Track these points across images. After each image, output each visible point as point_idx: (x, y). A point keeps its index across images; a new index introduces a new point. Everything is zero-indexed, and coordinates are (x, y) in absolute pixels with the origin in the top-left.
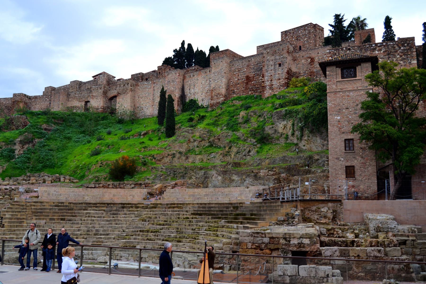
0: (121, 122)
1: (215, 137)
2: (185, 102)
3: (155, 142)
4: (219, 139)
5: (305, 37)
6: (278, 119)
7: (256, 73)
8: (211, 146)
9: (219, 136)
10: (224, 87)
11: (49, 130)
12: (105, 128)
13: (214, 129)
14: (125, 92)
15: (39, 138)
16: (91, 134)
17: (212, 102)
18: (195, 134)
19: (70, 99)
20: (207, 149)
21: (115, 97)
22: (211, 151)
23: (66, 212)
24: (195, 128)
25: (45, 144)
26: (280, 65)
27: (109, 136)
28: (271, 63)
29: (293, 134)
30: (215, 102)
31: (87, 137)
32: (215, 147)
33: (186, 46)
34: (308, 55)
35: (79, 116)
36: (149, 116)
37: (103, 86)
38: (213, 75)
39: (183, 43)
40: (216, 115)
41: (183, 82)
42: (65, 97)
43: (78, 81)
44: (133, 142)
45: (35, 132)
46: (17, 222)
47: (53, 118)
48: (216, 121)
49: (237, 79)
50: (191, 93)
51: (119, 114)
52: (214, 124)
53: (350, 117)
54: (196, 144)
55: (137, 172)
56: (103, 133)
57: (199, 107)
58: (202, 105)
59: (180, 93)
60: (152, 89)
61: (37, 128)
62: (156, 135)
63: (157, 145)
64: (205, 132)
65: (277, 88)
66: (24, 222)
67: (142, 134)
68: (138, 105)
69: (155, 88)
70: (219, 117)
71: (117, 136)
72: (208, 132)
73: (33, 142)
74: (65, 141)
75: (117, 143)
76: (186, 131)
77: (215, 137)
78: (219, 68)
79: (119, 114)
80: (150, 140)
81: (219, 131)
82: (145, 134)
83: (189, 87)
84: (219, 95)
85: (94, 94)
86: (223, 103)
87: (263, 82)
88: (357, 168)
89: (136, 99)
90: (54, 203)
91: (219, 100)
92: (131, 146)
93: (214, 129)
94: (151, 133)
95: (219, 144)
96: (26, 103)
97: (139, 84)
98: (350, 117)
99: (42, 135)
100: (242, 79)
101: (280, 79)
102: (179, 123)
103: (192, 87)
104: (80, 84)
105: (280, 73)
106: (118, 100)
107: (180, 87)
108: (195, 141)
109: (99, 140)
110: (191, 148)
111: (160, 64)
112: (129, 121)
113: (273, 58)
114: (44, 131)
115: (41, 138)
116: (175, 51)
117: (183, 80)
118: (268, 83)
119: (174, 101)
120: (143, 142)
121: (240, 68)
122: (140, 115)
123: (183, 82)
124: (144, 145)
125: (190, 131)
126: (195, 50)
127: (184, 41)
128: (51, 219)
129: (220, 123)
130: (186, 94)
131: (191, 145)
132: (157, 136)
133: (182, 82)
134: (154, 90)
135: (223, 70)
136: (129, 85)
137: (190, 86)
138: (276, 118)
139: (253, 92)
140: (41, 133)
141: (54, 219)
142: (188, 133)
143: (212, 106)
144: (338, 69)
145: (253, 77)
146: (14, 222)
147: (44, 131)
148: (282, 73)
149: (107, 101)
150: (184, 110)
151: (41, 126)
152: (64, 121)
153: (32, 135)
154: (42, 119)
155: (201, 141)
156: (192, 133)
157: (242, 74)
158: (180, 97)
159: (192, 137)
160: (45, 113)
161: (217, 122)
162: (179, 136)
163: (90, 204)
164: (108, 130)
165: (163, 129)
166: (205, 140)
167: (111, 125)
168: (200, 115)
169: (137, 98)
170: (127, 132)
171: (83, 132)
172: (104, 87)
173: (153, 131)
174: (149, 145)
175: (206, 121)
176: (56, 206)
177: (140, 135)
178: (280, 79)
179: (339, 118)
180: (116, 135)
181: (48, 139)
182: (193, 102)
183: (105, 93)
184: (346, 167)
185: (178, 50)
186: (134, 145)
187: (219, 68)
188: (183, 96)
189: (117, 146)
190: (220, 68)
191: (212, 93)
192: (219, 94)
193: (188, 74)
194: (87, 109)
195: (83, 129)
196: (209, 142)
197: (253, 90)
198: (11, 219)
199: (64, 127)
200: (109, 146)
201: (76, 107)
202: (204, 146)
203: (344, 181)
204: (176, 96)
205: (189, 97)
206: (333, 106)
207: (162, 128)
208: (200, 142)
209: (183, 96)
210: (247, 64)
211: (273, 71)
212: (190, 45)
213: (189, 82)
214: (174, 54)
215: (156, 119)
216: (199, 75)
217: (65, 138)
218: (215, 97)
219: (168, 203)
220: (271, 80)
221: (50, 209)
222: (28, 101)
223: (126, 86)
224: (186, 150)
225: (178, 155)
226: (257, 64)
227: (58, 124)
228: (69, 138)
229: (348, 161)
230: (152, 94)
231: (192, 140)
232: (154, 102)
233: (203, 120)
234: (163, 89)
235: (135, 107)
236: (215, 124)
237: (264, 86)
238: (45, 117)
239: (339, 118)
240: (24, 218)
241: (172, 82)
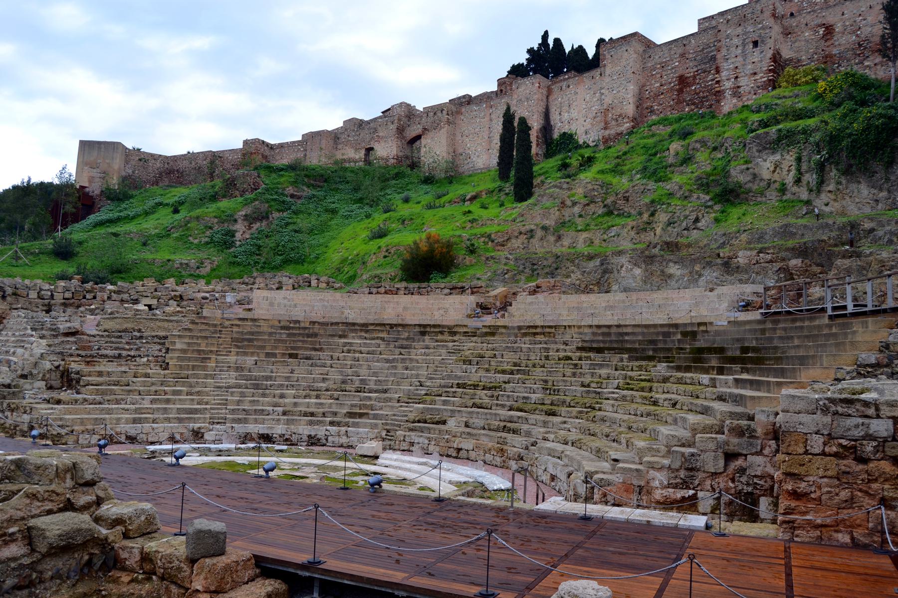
0: (429, 180)
1: (617, 195)
2: (551, 138)
3: (493, 211)
4: (627, 199)
6: (759, 151)
7: (699, 67)
8: (610, 213)
9: (627, 192)
10: (631, 101)
11: (299, 198)
12: (399, 193)
13: (615, 181)
14: (436, 126)
15: (279, 211)
16: (374, 203)
17: (607, 132)
18: (574, 191)
19: (340, 146)
20: (600, 220)
21: (418, 137)
22: (610, 224)
23: (303, 341)
24: (574, 180)
25: (290, 221)
26: (755, 44)
27: (406, 206)
28: (736, 41)
29: (798, 181)
30: (613, 132)
31: (367, 208)
32: (618, 215)
33: (551, 42)
34: (819, 21)
35: (352, 171)
36: (481, 169)
37: (396, 118)
38: (607, 79)
39: (545, 36)
40: (616, 155)
41: (547, 101)
42: (331, 142)
43: (357, 119)
44: (451, 213)
45: (273, 200)
46: (196, 359)
47: (306, 176)
48: (618, 165)
49: (658, 85)
50: (563, 120)
51: (426, 166)
52: (613, 171)
54: (577, 210)
55: (457, 267)
56: (397, 199)
57: (578, 147)
58: (584, 143)
59: (542, 122)
60: (487, 119)
61: (276, 193)
62: (495, 198)
63: (498, 216)
64: (596, 187)
65: (750, 93)
66: (210, 358)
67: (468, 198)
68: (461, 151)
69: (493, 116)
70: (624, 157)
71: (420, 205)
72: (602, 187)
73: (268, 218)
74: (325, 217)
75: (419, 215)
76: (555, 186)
77: (617, 195)
78: (622, 64)
79: (426, 166)
80: (484, 207)
81: (627, 184)
82: (473, 198)
83: (558, 110)
85: (381, 134)
86: (630, 133)
87: (718, 82)
89: (457, 139)
90: (279, 321)
91: (622, 129)
92: (445, 219)
93: (615, 181)
94: (484, 196)
95: (626, 209)
96: (265, 157)
97: (463, 110)
99: (284, 206)
100: (670, 83)
101: (755, 74)
102: (540, 175)
103: (565, 108)
104: (361, 125)
105: (756, 60)
106: (423, 141)
107: (542, 109)
108: (574, 204)
109: (386, 212)
110: (567, 219)
111: (505, 74)
112: (445, 178)
113: (739, 30)
114: (289, 199)
115: (283, 211)
116: (530, 51)
117: (547, 97)
118: (728, 85)
119: (530, 129)
120: (469, 212)
121: (665, 62)
122: (465, 168)
123: (547, 101)
124: (470, 217)
125: (565, 186)
126: (568, 49)
127: (546, 33)
128: (268, 355)
129: (625, 168)
130: (552, 123)
131: (567, 213)
132: (496, 200)
133: (545, 100)
134: (491, 120)
135: (629, 68)
136: (445, 112)
137: (561, 107)
138: (754, 150)
139: (693, 107)
140: (283, 202)
141: (274, 355)
142: (561, 188)
143: (606, 140)
145: (694, 77)
146: (189, 359)
147: (289, 199)
148: (761, 61)
149: (405, 146)
150: (548, 155)
151: (284, 189)
152: (325, 181)
153: (267, 205)
154: (288, 177)
155: (588, 205)
156: (569, 189)
157: (669, 72)
158: (541, 129)
159: (569, 197)
160: (292, 167)
161: (619, 168)
162: (542, 196)
163: (354, 324)
164: (406, 193)
165: (509, 187)
166: (595, 202)
167: (410, 186)
168: (583, 157)
169: (459, 137)
170: (439, 197)
171: (360, 200)
172: (399, 120)
173: (490, 192)
174: (481, 217)
175: (595, 168)
176: (283, 328)
177: (464, 201)
178: (755, 74)
180: (419, 203)
181: (296, 213)
182: (568, 141)
183: (401, 131)
185: (536, 49)
186: (453, 216)
187: (622, 64)
188: (547, 128)
189: (419, 221)
190: (624, 63)
191: (606, 116)
192: (620, 116)
193: (557, 85)
194: (367, 161)
195: (359, 195)
196: (605, 206)
197: (694, 104)
198: (184, 351)
199: (325, 191)
200: (404, 221)
201: (349, 161)
202: (594, 213)
204: (535, 124)
205: (559, 127)
207: (508, 185)
208: (585, 206)
209: (547, 128)
210: (680, 51)
211: (740, 59)
212: (557, 41)
213: (558, 98)
214: (528, 56)
215: (494, 173)
216: (579, 83)
217: (327, 211)
218: (614, 123)
219: (522, 324)
220: (737, 77)
221: (270, 334)
222: (267, 153)
223: (439, 114)
224: (556, 223)
225: (539, 233)
226: (703, 49)
227: (314, 187)
228: (334, 212)
230: (486, 129)
231: (569, 203)
232: (490, 142)
233: (589, 166)
234: (508, 109)
235: (455, 154)
236: (616, 171)
237: (719, 92)
238: (293, 174)
240: (211, 351)
241: (528, 101)
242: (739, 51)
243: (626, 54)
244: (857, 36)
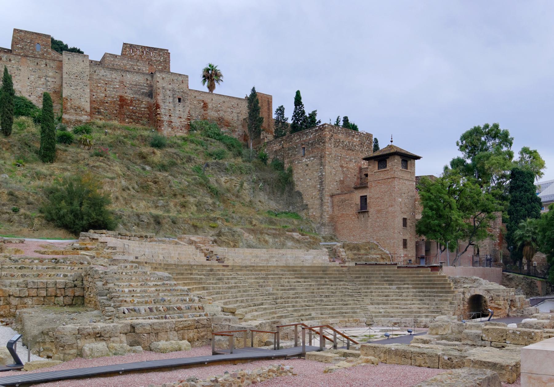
5: (159, 65)
7: (135, 96)
26: (180, 100)
28: (168, 92)
84: (79, 110)
88: (408, 241)
121: (108, 81)
157: (112, 89)
192: (79, 108)
197: (132, 119)
203: (402, 251)
211: (171, 105)
220: (170, 116)
242: (171, 100)
243: (82, 63)
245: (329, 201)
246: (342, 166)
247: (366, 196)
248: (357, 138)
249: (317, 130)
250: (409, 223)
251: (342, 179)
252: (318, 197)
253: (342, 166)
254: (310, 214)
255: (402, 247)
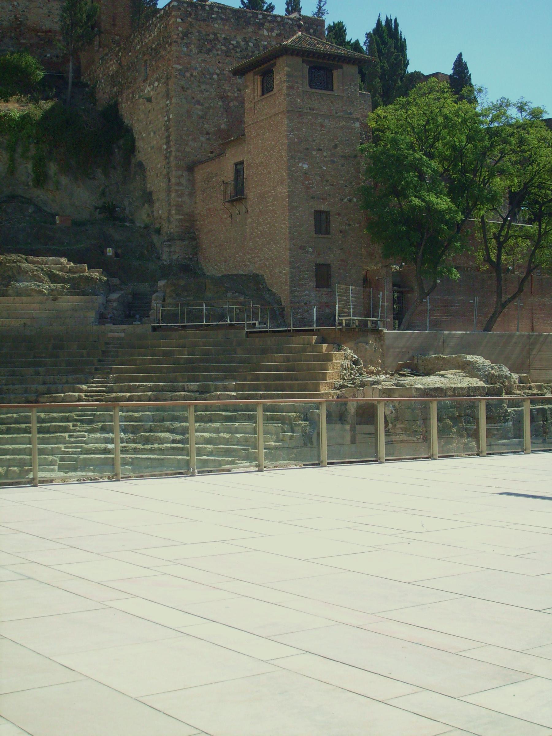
53: (325, 168)
98: (325, 168)
144: (305, 65)
179: (306, 166)
184: (318, 265)
206: (296, 140)
229: (319, 254)
239: (306, 166)
244: (13, 6)
245: (183, 181)
246: (223, 97)
247: (242, 163)
248: (271, 30)
249: (162, 16)
250: (335, 224)
251: (223, 127)
252: (165, 172)
253: (223, 97)
254: (156, 214)
255: (313, 284)
